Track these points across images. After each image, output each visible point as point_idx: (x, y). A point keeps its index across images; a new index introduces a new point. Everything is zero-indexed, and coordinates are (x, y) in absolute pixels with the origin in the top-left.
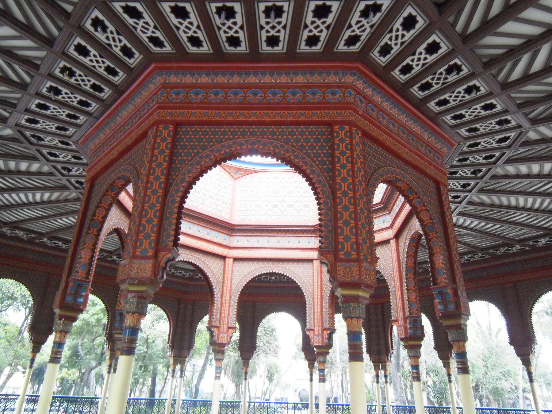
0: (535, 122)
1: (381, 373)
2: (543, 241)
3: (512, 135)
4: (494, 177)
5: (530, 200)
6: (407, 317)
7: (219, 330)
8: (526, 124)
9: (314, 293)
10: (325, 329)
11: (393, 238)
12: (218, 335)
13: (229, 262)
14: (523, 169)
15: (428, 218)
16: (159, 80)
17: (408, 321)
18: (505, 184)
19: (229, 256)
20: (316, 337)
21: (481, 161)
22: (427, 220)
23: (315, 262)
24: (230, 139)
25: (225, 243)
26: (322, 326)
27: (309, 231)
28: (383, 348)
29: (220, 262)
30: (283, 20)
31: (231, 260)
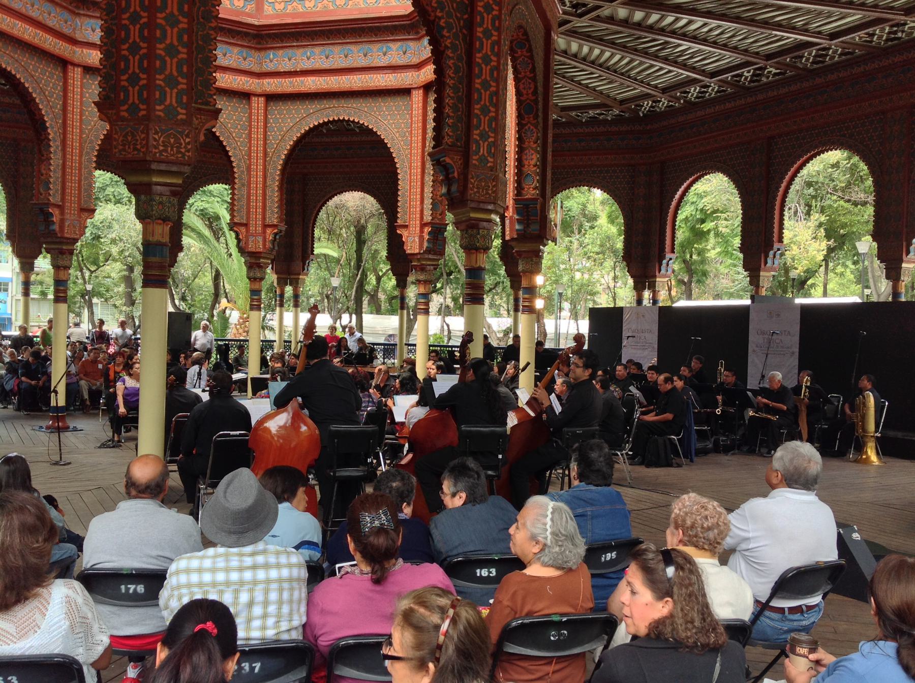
1: (289, 290)
4: (598, 19)
6: (426, 224)
7: (62, 213)
9: (250, 159)
10: (269, 226)
11: (418, 88)
12: (62, 221)
13: (76, 74)
15: (530, 92)
17: (427, 230)
19: (76, 61)
20: (251, 239)
22: (527, 94)
23: (254, 99)
25: (67, 31)
26: (264, 218)
27: (246, 35)
28: (298, 253)
29: (58, 73)
31: (79, 70)
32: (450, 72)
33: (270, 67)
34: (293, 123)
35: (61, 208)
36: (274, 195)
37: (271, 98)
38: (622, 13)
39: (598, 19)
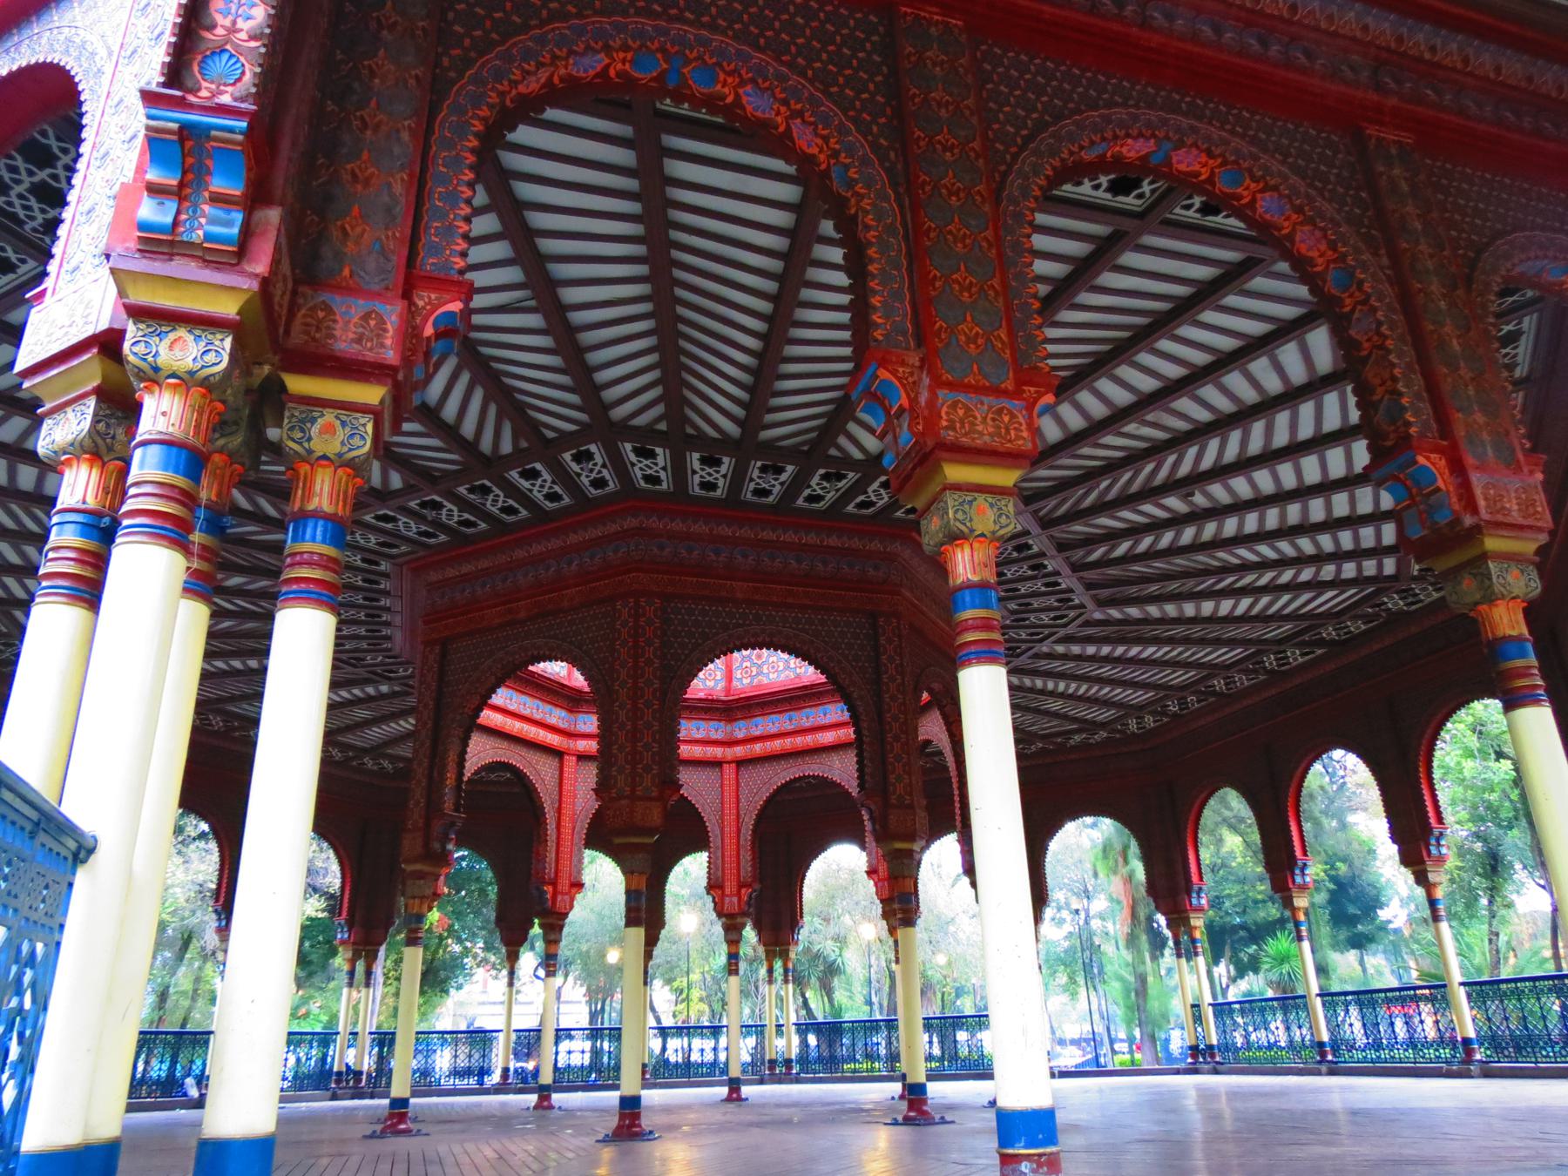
0: (1102, 603)
2: (1077, 738)
3: (1072, 614)
4: (1037, 656)
5: (1073, 685)
8: (1090, 605)
13: (570, 761)
14: (1076, 649)
16: (630, 522)
18: (1043, 664)
21: (1024, 636)
24: (738, 626)
30: (840, 485)
32: (865, 732)
33: (740, 735)
34: (762, 784)
35: (554, 884)
36: (746, 856)
37: (740, 763)
38: (1060, 649)
39: (1037, 656)
